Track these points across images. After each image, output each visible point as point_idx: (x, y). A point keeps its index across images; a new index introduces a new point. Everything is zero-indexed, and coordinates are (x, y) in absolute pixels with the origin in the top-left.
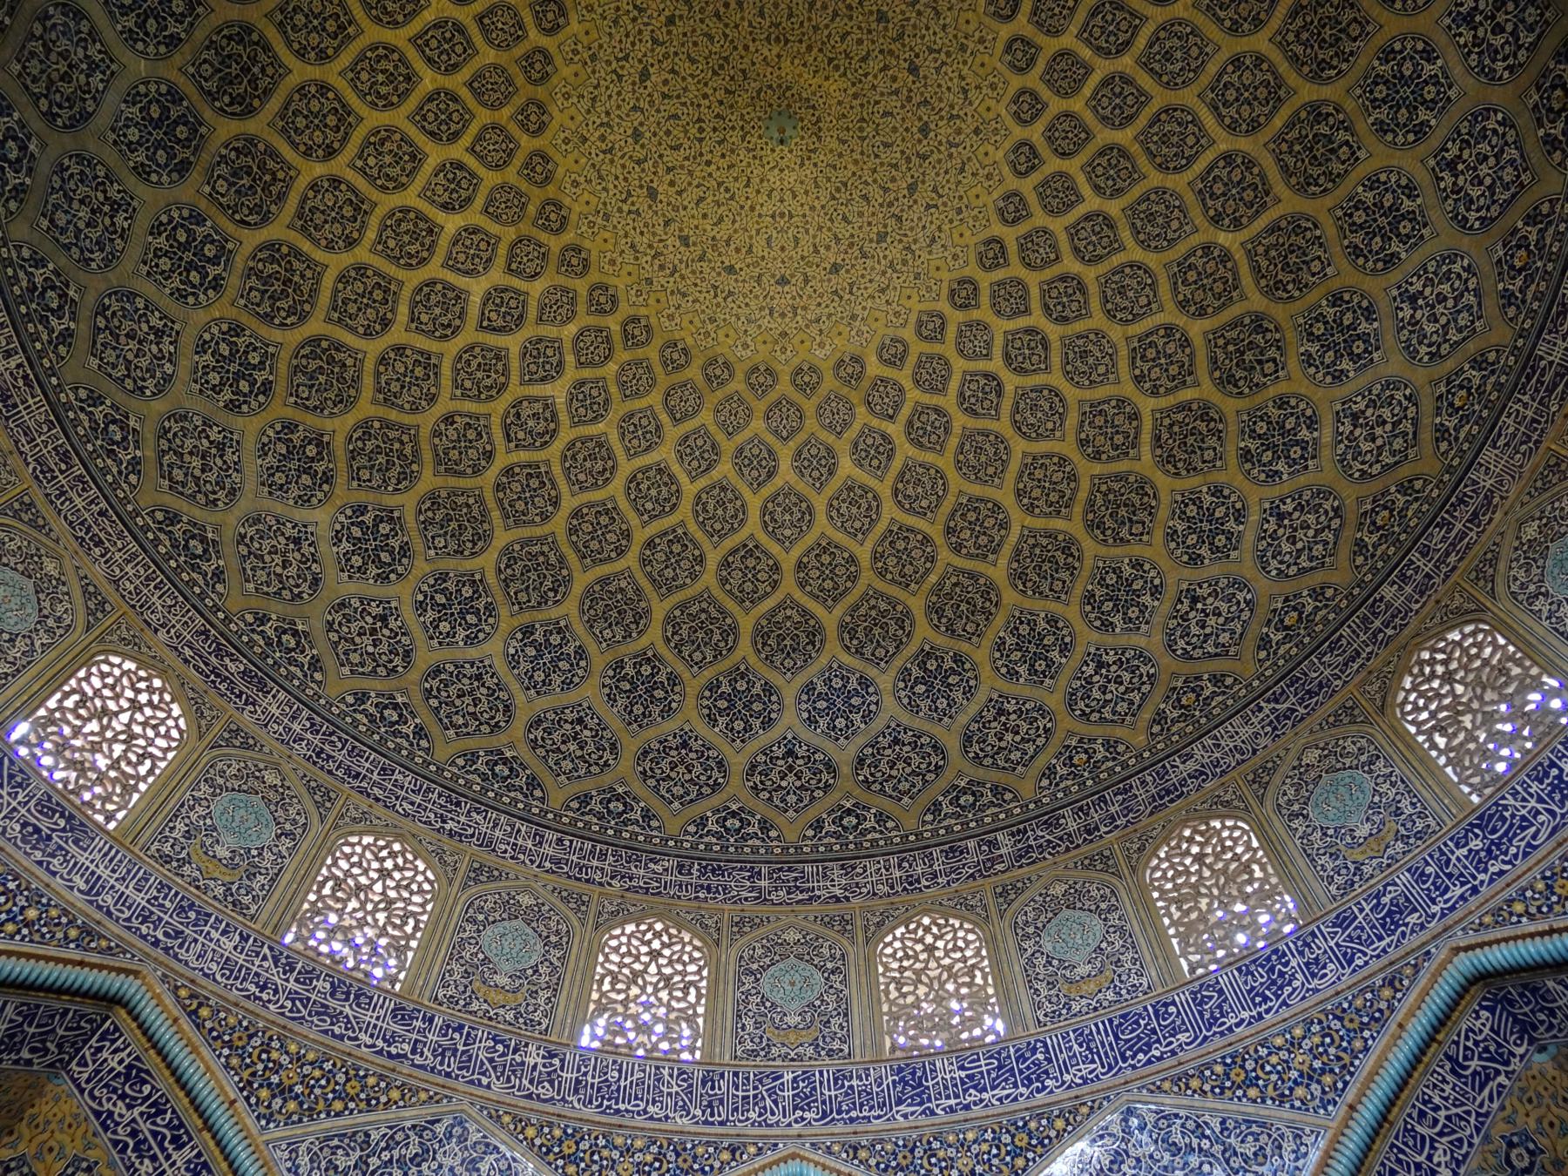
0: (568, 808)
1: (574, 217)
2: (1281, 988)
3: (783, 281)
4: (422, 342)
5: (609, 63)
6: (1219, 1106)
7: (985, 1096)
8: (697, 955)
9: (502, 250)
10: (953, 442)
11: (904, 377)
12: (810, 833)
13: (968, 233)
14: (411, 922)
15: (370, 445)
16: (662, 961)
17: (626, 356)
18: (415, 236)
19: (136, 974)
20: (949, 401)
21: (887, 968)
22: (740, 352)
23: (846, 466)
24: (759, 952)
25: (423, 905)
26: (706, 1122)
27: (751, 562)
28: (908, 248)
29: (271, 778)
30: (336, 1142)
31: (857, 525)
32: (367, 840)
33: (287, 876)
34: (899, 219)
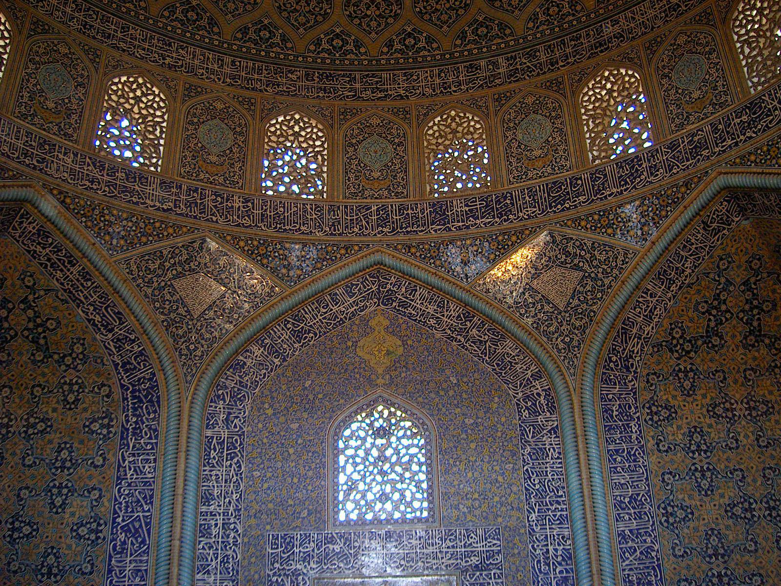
0: (236, 39)
2: (635, 178)
6: (592, 236)
7: (478, 221)
8: (320, 134)
12: (385, 50)
14: (158, 128)
16: (301, 139)
19: (30, 186)
21: (429, 144)
24: (356, 131)
25: (162, 117)
26: (332, 234)
29: (64, 50)
30: (147, 257)
32: (124, 79)
33: (87, 112)
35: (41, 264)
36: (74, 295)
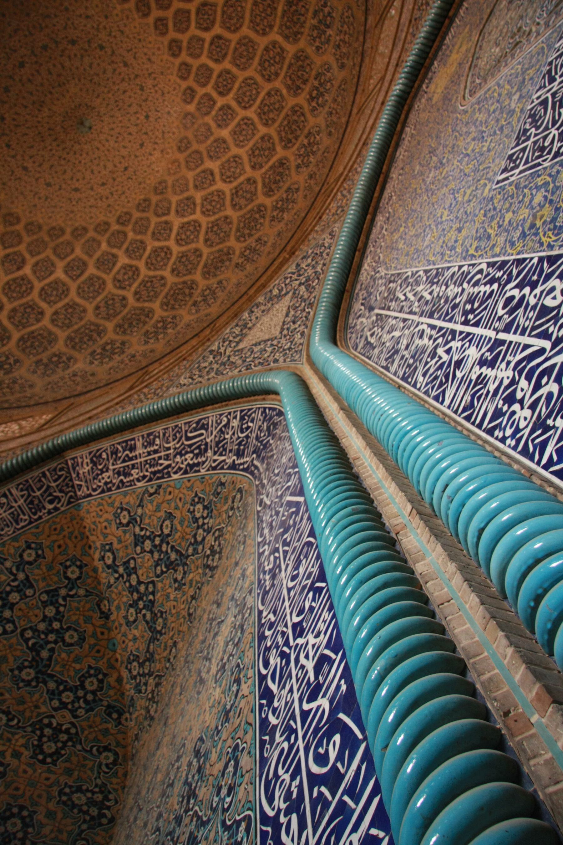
1: (63, 225)
3: (142, 145)
4: (60, 305)
5: (10, 180)
9: (53, 257)
10: (234, 70)
11: (201, 91)
13: (150, 39)
15: (77, 340)
17: (130, 227)
18: (20, 286)
22: (158, 175)
23: (225, 133)
27: (241, 193)
28: (150, 74)
31: (250, 132)
34: (137, 76)
35: (118, 488)
36: (159, 471)
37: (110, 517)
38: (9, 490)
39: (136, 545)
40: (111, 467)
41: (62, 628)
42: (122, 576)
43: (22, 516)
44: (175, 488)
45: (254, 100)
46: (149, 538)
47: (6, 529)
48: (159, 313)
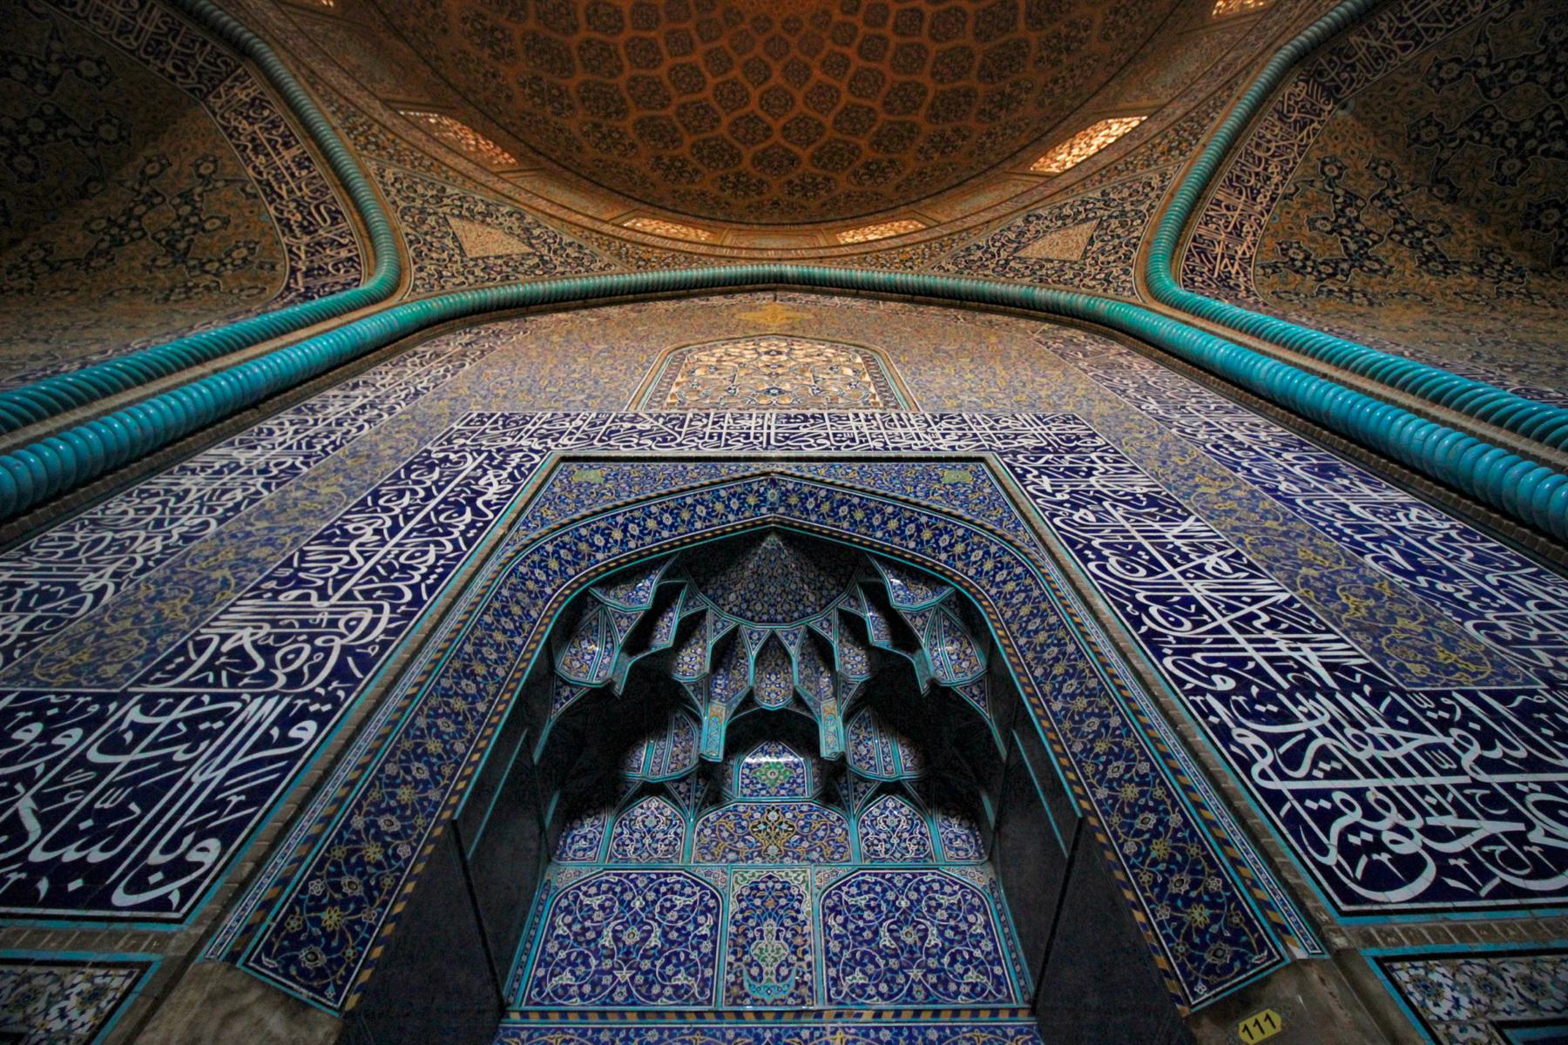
10: (889, 54)
20: (887, 31)
23: (817, 74)
35: (237, 146)
36: (272, 188)
37: (201, 151)
38: (153, 6)
39: (180, 196)
40: (256, 127)
41: (26, 149)
42: (139, 193)
43: (132, 38)
44: (259, 215)
45: (860, 96)
46: (194, 208)
47: (100, 24)
48: (572, 84)
